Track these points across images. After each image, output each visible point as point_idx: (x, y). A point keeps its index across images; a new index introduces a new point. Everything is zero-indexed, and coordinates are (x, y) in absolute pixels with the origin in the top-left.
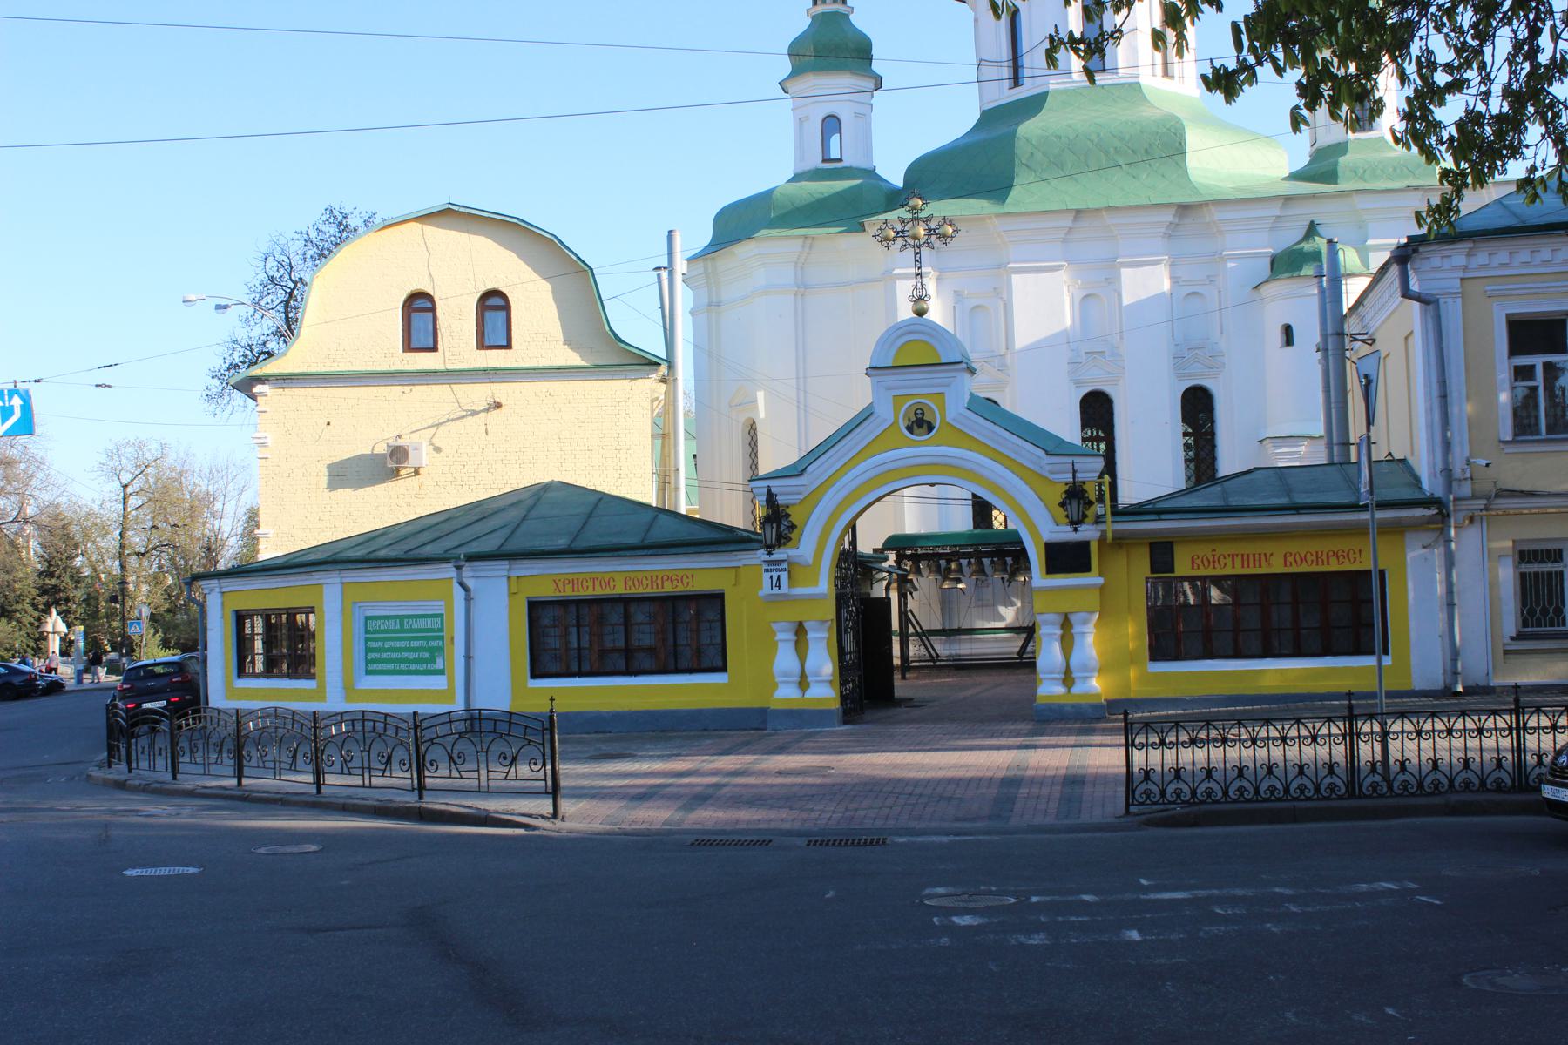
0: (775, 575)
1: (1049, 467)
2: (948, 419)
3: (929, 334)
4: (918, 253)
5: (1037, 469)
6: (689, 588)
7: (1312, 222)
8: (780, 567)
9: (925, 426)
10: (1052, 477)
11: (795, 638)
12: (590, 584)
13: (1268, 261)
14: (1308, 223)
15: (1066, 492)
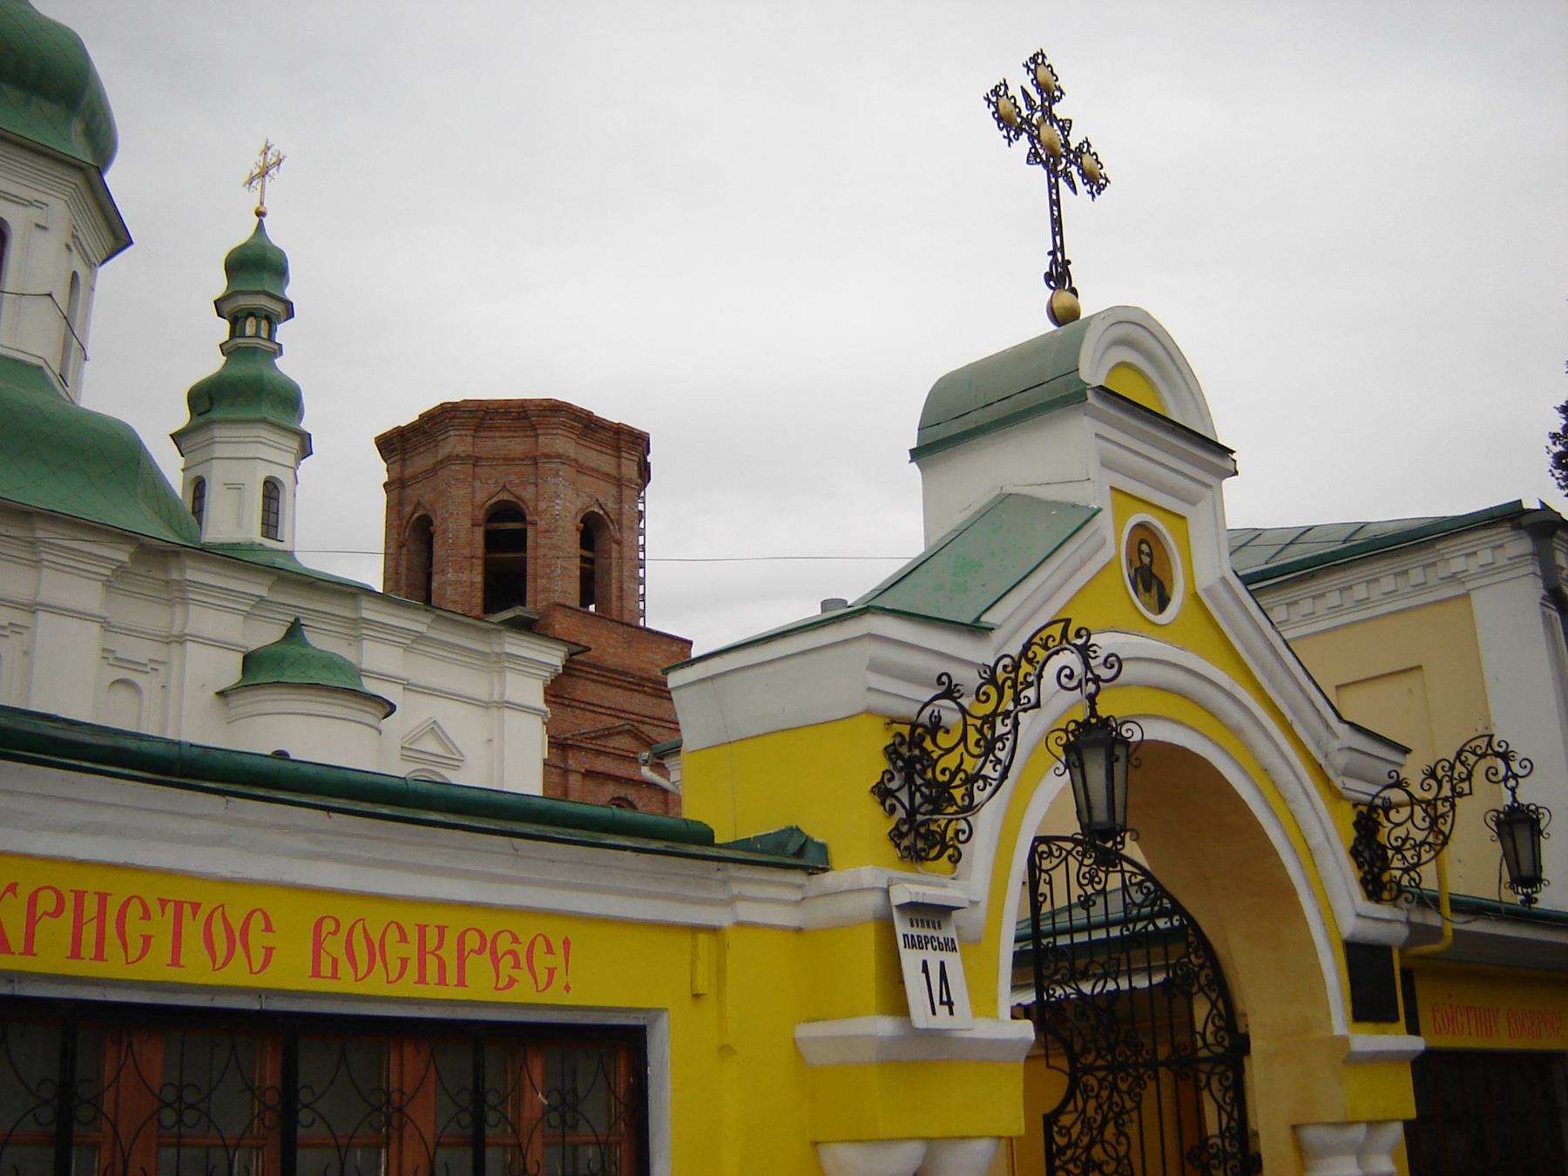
0: (933, 958)
1: (1341, 760)
3: (1159, 367)
5: (1321, 761)
6: (555, 996)
7: (297, 620)
8: (941, 935)
9: (1154, 590)
10: (1338, 782)
12: (161, 927)
13: (240, 657)
14: (292, 620)
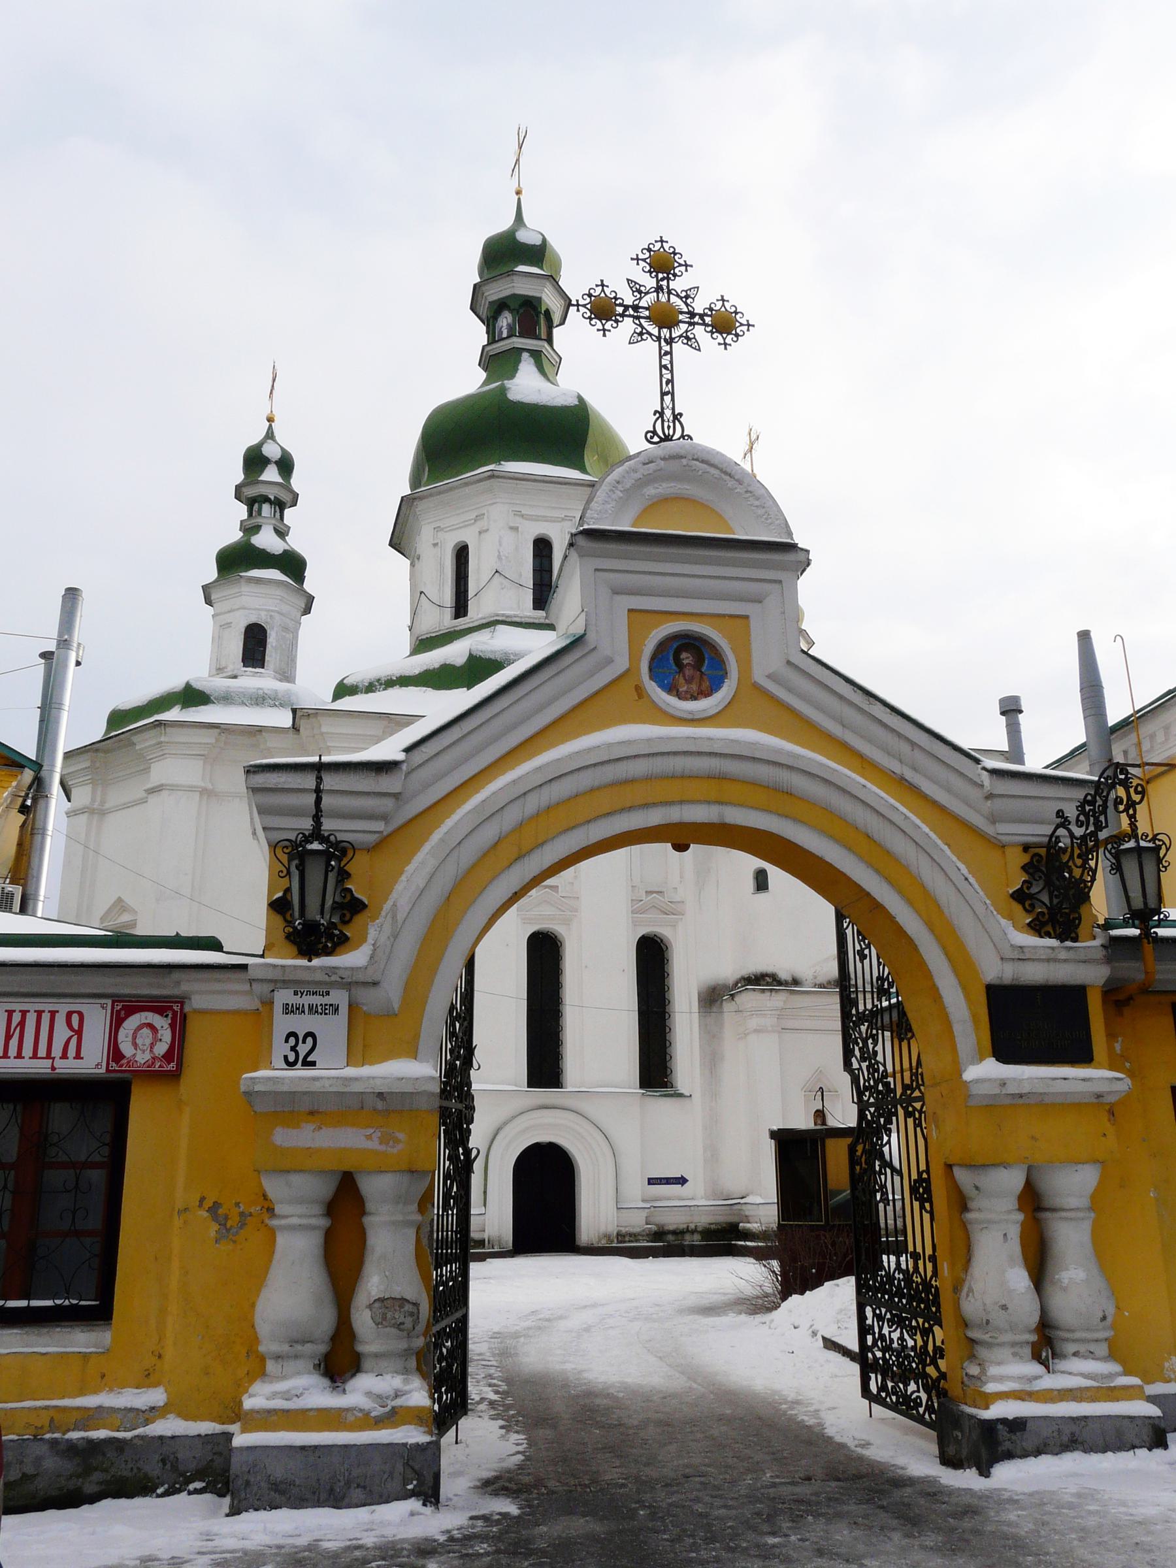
2: (759, 676)
4: (666, 353)
10: (990, 830)
11: (324, 1222)
15: (1024, 868)
